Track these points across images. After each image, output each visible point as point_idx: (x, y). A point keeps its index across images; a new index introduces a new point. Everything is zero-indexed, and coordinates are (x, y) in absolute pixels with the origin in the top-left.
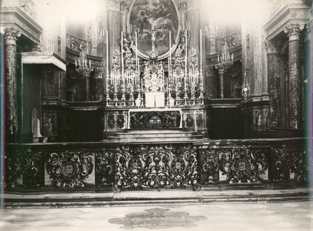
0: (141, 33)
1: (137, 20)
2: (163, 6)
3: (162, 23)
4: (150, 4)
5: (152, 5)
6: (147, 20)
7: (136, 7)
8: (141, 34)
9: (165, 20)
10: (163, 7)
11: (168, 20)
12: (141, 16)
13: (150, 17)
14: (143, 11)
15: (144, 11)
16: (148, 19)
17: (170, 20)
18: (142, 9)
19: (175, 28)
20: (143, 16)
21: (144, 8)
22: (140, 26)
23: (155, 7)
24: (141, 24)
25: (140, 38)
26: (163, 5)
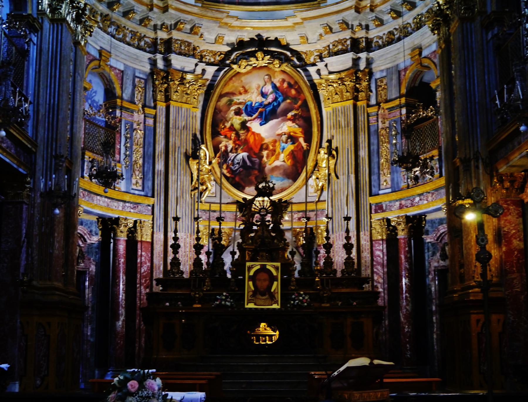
0: (234, 151)
1: (226, 124)
2: (280, 96)
3: (279, 132)
4: (253, 93)
5: (258, 96)
6: (248, 124)
7: (225, 100)
8: (235, 154)
9: (284, 125)
10: (280, 99)
11: (290, 123)
12: (235, 117)
13: (254, 119)
14: (239, 108)
15: (241, 106)
16: (249, 122)
17: (294, 124)
18: (236, 104)
19: (305, 142)
20: (238, 117)
21: (241, 101)
22: (233, 138)
23: (264, 100)
24: (234, 132)
25: (233, 161)
26: (280, 94)
